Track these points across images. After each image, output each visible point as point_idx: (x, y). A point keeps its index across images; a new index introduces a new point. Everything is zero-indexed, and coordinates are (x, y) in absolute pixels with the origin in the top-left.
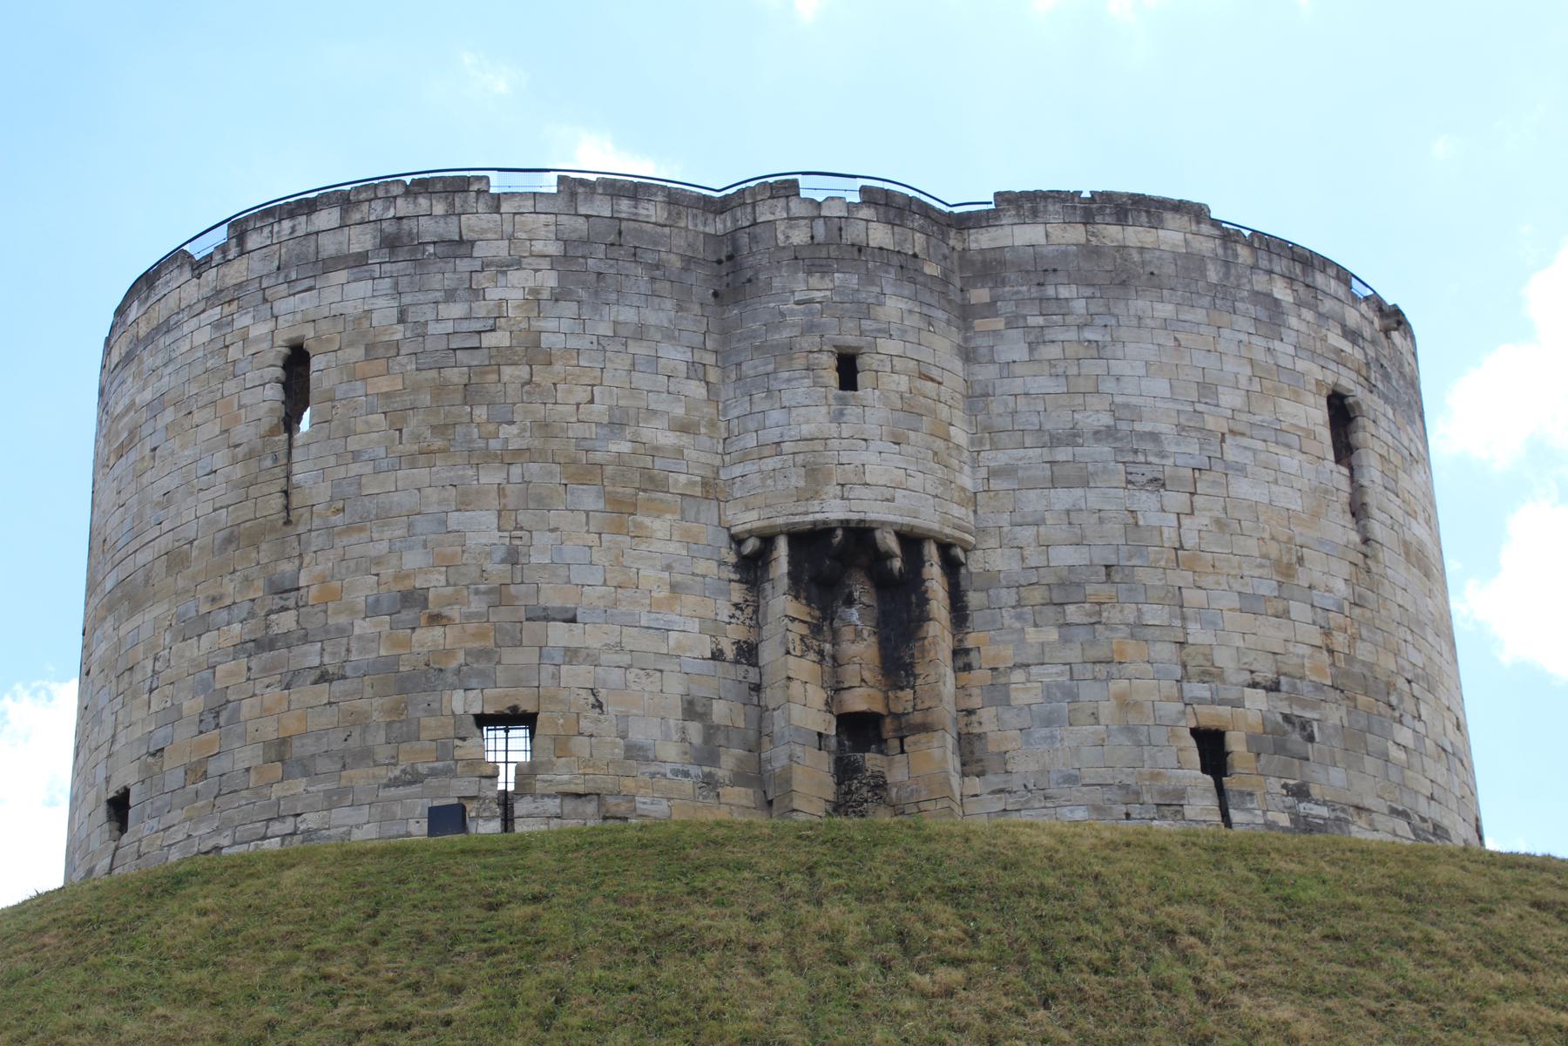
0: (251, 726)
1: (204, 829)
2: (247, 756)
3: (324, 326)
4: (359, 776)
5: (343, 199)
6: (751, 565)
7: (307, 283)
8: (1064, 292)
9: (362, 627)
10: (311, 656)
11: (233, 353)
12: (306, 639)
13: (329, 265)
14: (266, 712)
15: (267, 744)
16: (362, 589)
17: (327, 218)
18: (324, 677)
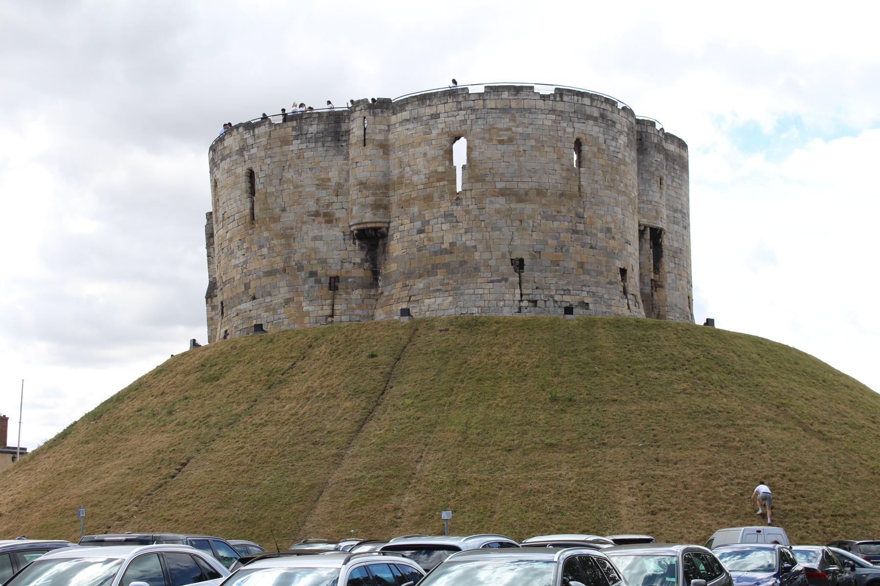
0: (573, 256)
1: (561, 282)
2: (572, 264)
3: (588, 136)
4: (600, 278)
5: (593, 97)
6: (641, 233)
7: (583, 121)
8: (677, 167)
9: (600, 235)
10: (588, 240)
11: (560, 133)
12: (587, 234)
13: (589, 117)
14: (577, 253)
15: (578, 263)
16: (599, 224)
17: (587, 101)
18: (591, 247)
